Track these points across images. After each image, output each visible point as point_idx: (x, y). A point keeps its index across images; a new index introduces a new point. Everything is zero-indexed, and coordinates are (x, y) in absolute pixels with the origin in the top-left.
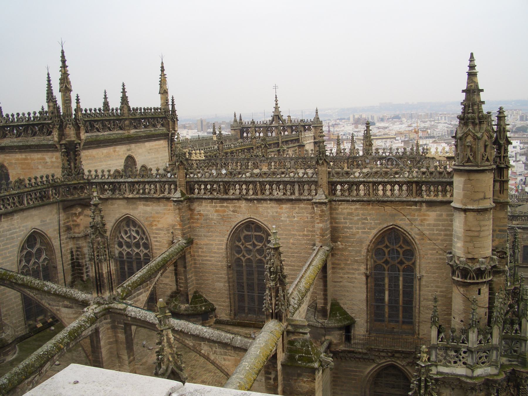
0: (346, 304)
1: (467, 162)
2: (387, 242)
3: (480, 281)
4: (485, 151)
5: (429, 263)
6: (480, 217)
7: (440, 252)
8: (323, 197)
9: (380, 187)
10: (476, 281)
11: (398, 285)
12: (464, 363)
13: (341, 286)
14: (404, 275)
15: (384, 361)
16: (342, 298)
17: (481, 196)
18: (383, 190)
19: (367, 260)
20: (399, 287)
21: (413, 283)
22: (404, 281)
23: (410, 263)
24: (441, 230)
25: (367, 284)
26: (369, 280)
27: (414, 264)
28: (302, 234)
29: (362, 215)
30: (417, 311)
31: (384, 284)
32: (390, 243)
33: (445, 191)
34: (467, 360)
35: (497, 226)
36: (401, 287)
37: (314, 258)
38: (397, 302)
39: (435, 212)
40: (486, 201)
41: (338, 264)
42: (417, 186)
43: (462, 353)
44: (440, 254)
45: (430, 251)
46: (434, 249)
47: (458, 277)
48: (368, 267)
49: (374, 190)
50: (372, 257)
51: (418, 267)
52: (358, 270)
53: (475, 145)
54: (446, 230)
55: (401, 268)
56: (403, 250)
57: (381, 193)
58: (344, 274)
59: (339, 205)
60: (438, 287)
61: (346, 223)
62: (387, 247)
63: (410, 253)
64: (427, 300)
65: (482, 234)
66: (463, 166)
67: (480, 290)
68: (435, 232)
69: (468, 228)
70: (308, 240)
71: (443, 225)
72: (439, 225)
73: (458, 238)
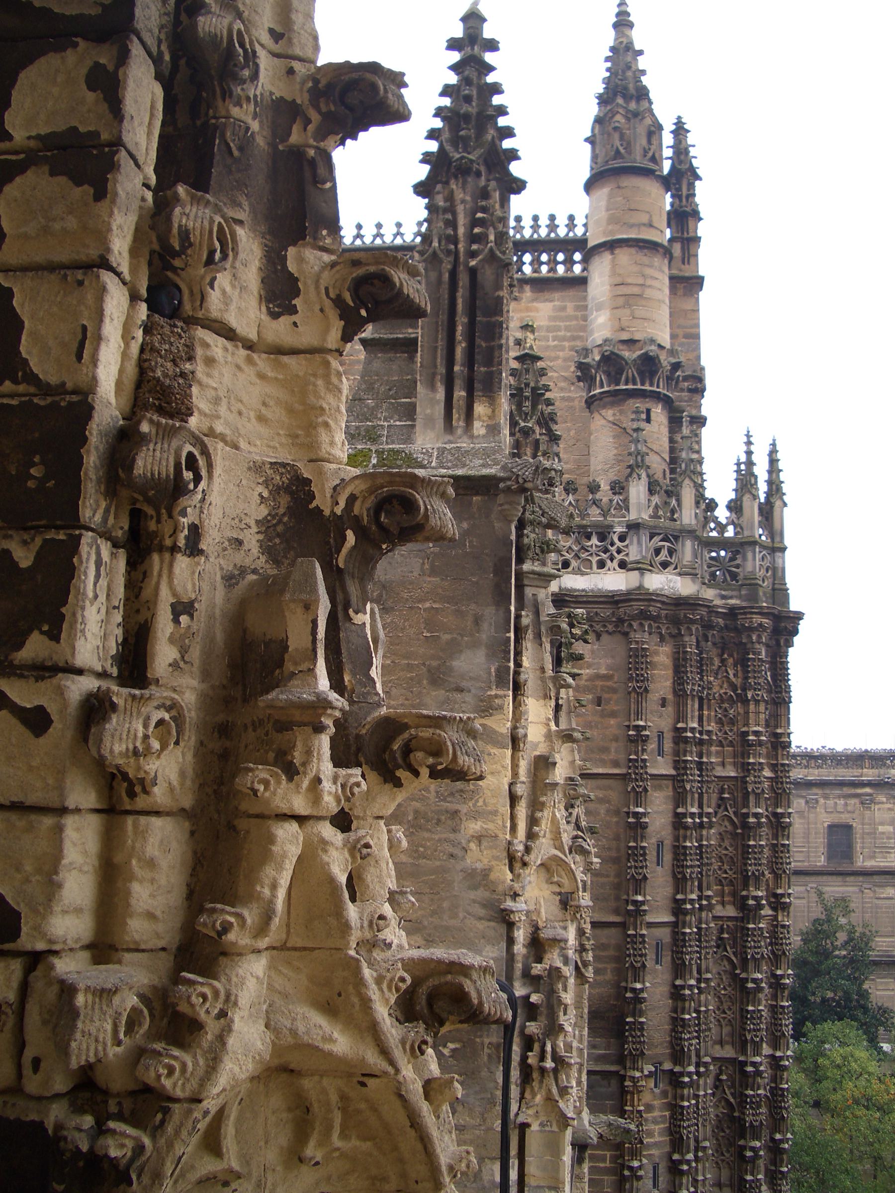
3: (647, 387)
7: (563, 384)
10: (639, 387)
12: (623, 565)
24: (563, 339)
34: (627, 555)
35: (679, 327)
39: (551, 301)
43: (616, 540)
44: (562, 389)
53: (629, 129)
54: (574, 338)
67: (648, 411)
71: (567, 329)
72: (558, 329)
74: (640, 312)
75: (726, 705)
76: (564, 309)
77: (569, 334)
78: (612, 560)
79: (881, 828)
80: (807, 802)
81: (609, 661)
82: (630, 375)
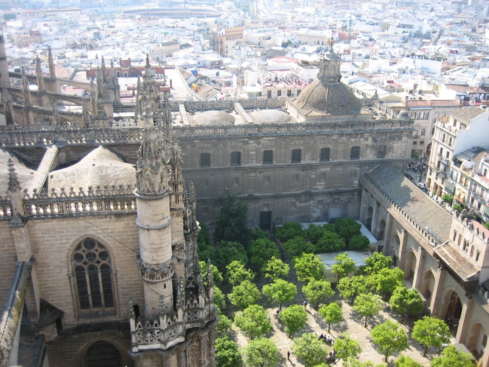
0: (53, 300)
1: (147, 192)
2: (83, 248)
4: (162, 182)
5: (122, 261)
6: (160, 233)
7: (131, 252)
8: (20, 220)
9: (73, 205)
10: (161, 280)
11: (98, 279)
12: (159, 340)
13: (47, 288)
14: (101, 271)
15: (93, 339)
16: (49, 296)
17: (161, 217)
18: (75, 207)
19: (68, 264)
20: (98, 281)
21: (110, 276)
22: (102, 275)
23: (106, 262)
24: (130, 235)
25: (70, 282)
26: (72, 279)
27: (109, 261)
28: (3, 249)
29: (59, 229)
30: (116, 297)
31: (85, 280)
32: (86, 247)
33: (129, 205)
36: (100, 280)
37: (19, 279)
38: (98, 292)
39: (123, 221)
40: (164, 220)
41: (43, 271)
42: (105, 202)
43: (156, 334)
44: (130, 253)
45: (122, 252)
46: (125, 250)
47: (147, 277)
48: (70, 270)
49: (67, 207)
50: (72, 261)
51: (113, 264)
52: (61, 273)
53: (153, 178)
55: (99, 266)
56: (99, 252)
57: (73, 209)
58: (49, 278)
59: (36, 223)
60: (131, 278)
61: (44, 237)
62: (84, 251)
63: (105, 255)
64: (123, 288)
65: (163, 245)
66: (144, 195)
67: (165, 285)
68: (125, 237)
69: (151, 243)
70: (10, 254)
71: (130, 231)
72: (127, 232)
73: (145, 249)
74: (160, 254)
75: (194, 351)
76: (129, 224)
77: (131, 233)
78: (155, 339)
79: (251, 153)
80: (223, 145)
81: (156, 364)
82: (158, 277)
